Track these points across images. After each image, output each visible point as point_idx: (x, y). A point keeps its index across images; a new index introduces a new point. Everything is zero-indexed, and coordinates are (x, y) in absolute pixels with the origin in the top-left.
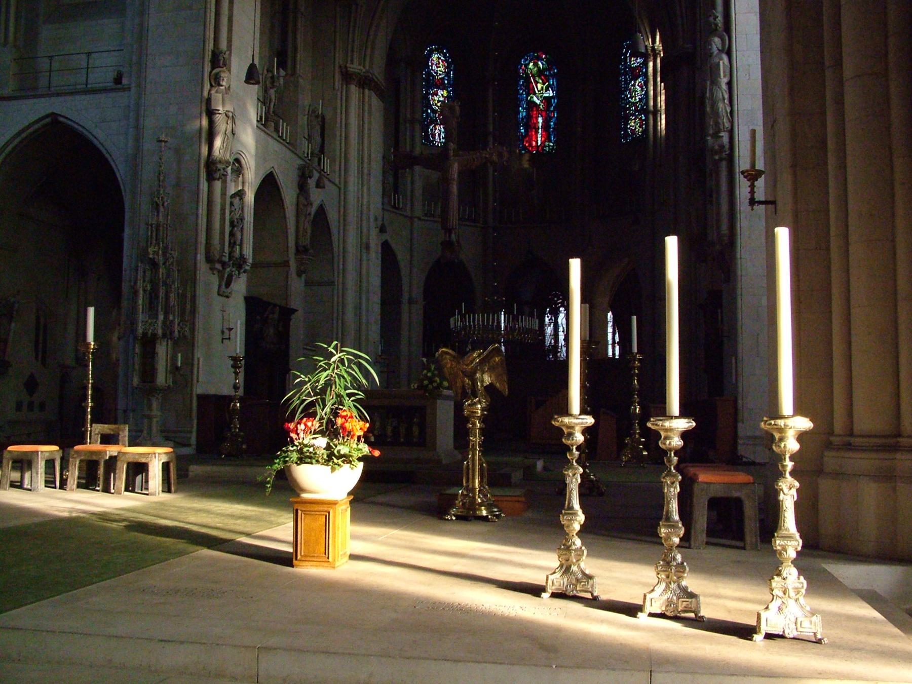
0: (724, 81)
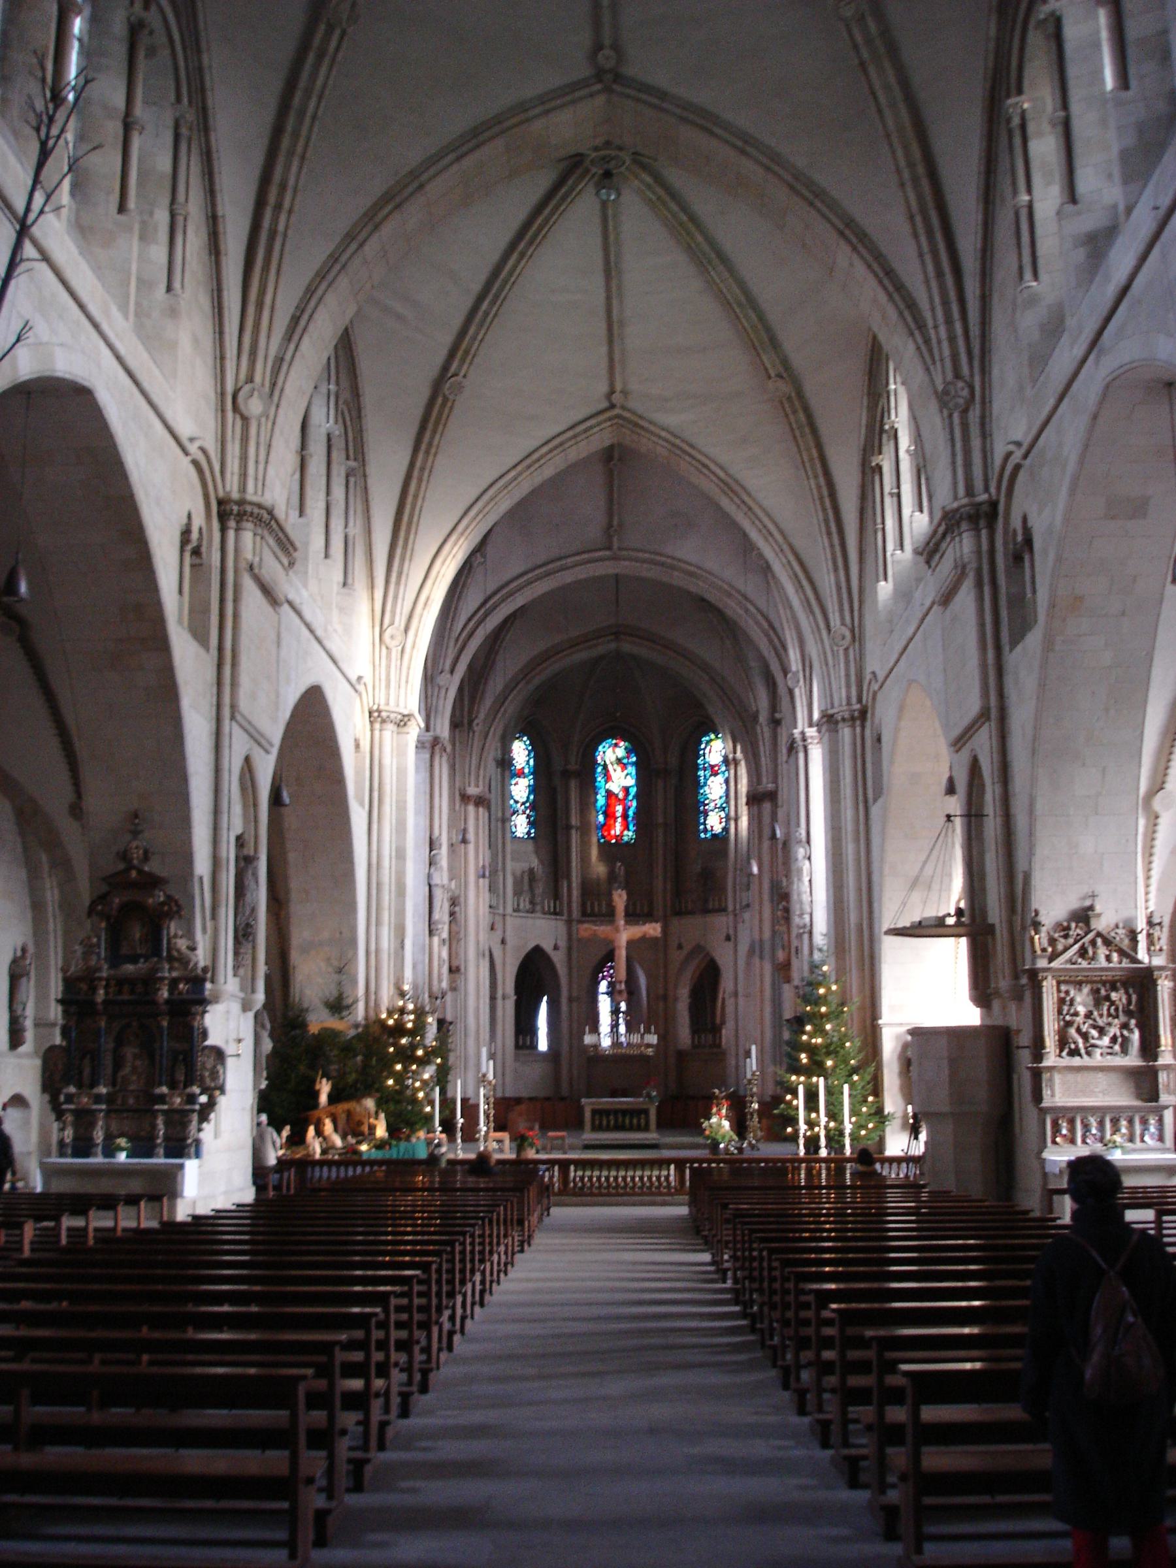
0: (806, 879)
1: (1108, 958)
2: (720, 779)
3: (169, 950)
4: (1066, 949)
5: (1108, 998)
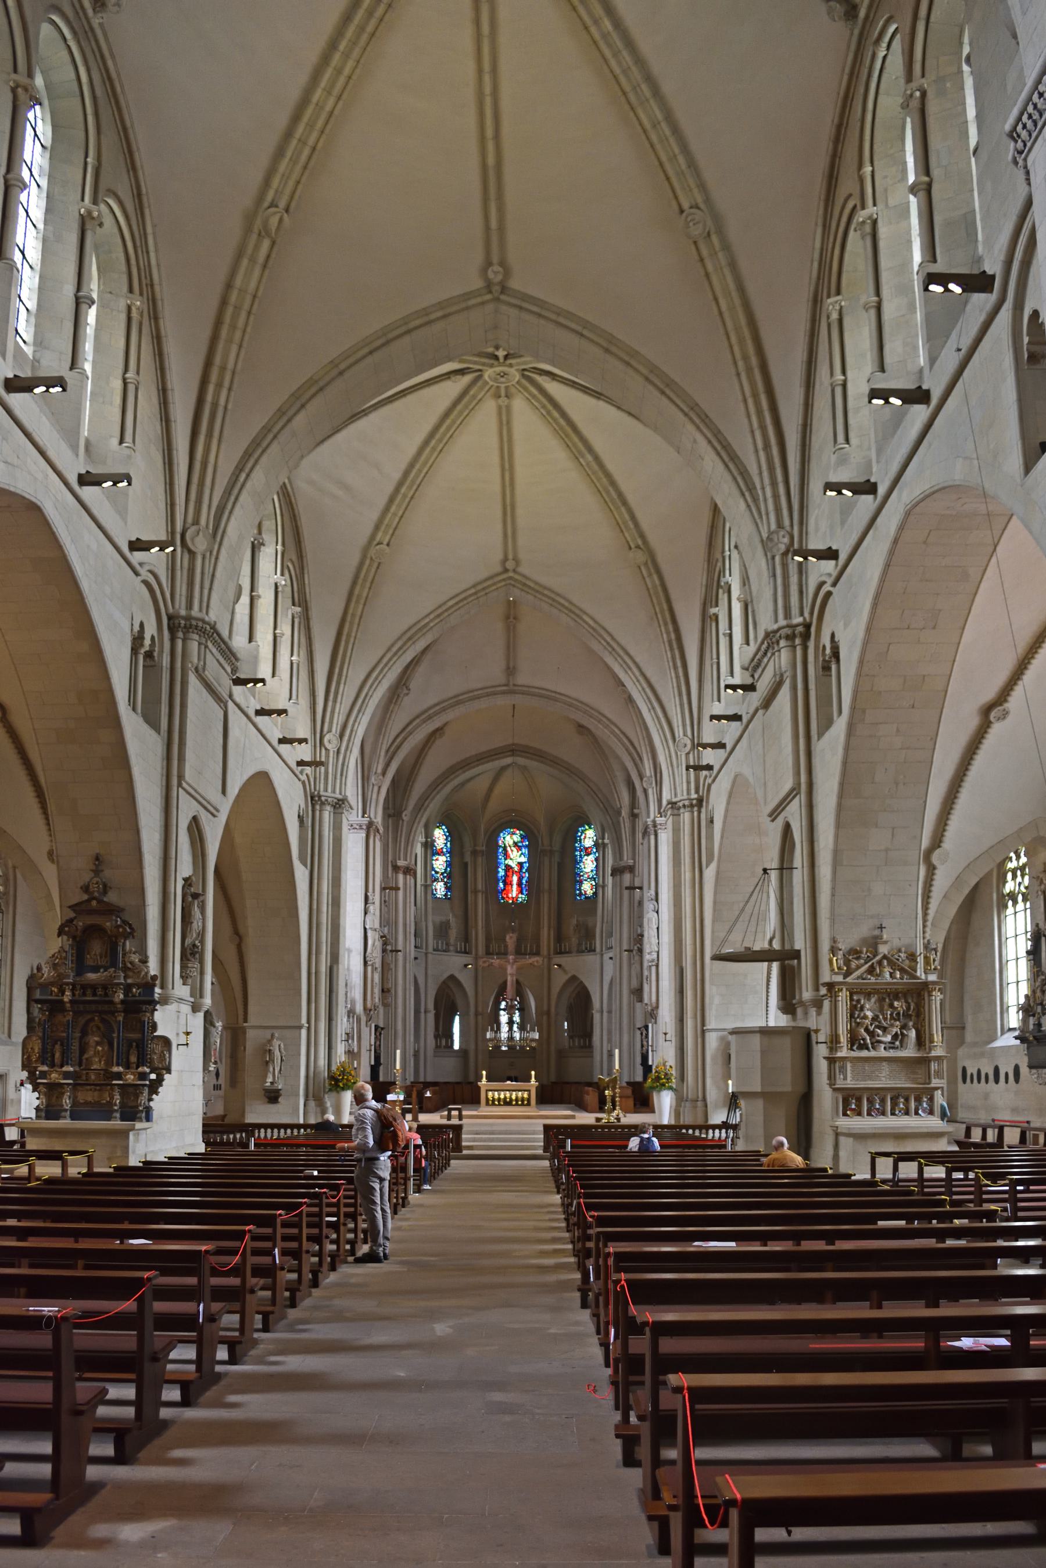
1: (891, 974)
2: (592, 857)
3: (124, 962)
4: (858, 967)
5: (891, 1006)
